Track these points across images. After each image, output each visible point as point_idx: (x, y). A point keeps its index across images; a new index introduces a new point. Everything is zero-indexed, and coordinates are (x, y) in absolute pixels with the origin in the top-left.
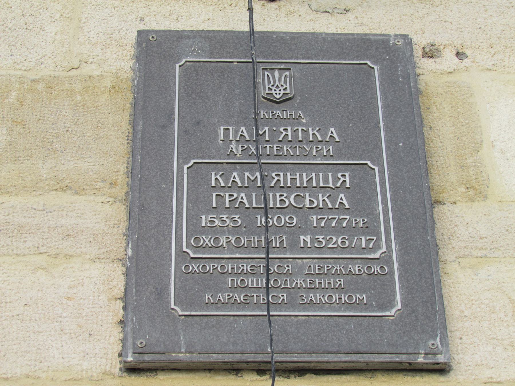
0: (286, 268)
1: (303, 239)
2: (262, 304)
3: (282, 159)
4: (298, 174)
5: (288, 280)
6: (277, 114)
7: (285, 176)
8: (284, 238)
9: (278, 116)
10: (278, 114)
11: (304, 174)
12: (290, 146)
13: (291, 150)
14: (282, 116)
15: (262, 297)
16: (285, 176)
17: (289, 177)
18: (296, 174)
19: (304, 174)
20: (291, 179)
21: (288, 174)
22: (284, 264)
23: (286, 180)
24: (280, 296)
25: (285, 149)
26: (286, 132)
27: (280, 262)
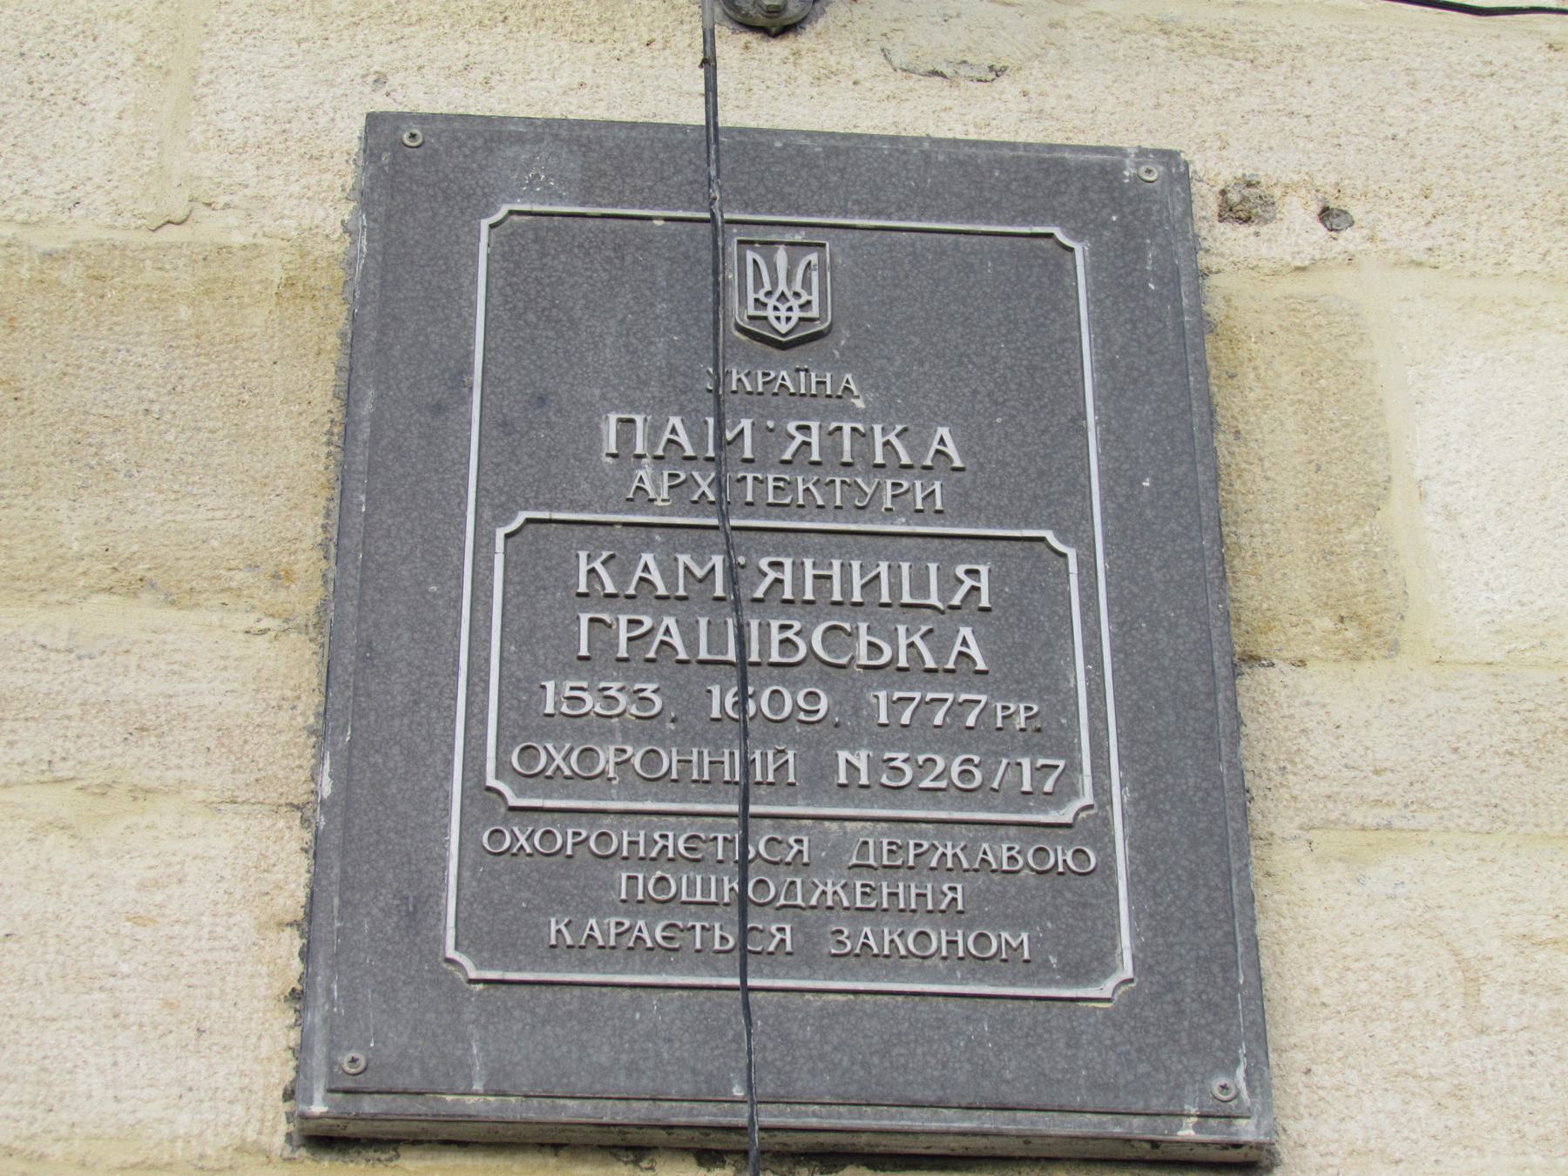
0: (792, 847)
1: (847, 761)
2: (719, 952)
3: (790, 518)
4: (836, 564)
5: (799, 882)
6: (779, 381)
7: (798, 567)
8: (790, 755)
9: (781, 385)
10: (783, 379)
11: (856, 565)
12: (815, 478)
13: (818, 490)
14: (794, 386)
15: (718, 933)
16: (798, 567)
17: (809, 572)
18: (831, 564)
19: (856, 565)
20: (816, 577)
21: (808, 563)
22: (789, 833)
23: (800, 582)
24: (773, 929)
25: (801, 487)
26: (805, 435)
27: (775, 829)
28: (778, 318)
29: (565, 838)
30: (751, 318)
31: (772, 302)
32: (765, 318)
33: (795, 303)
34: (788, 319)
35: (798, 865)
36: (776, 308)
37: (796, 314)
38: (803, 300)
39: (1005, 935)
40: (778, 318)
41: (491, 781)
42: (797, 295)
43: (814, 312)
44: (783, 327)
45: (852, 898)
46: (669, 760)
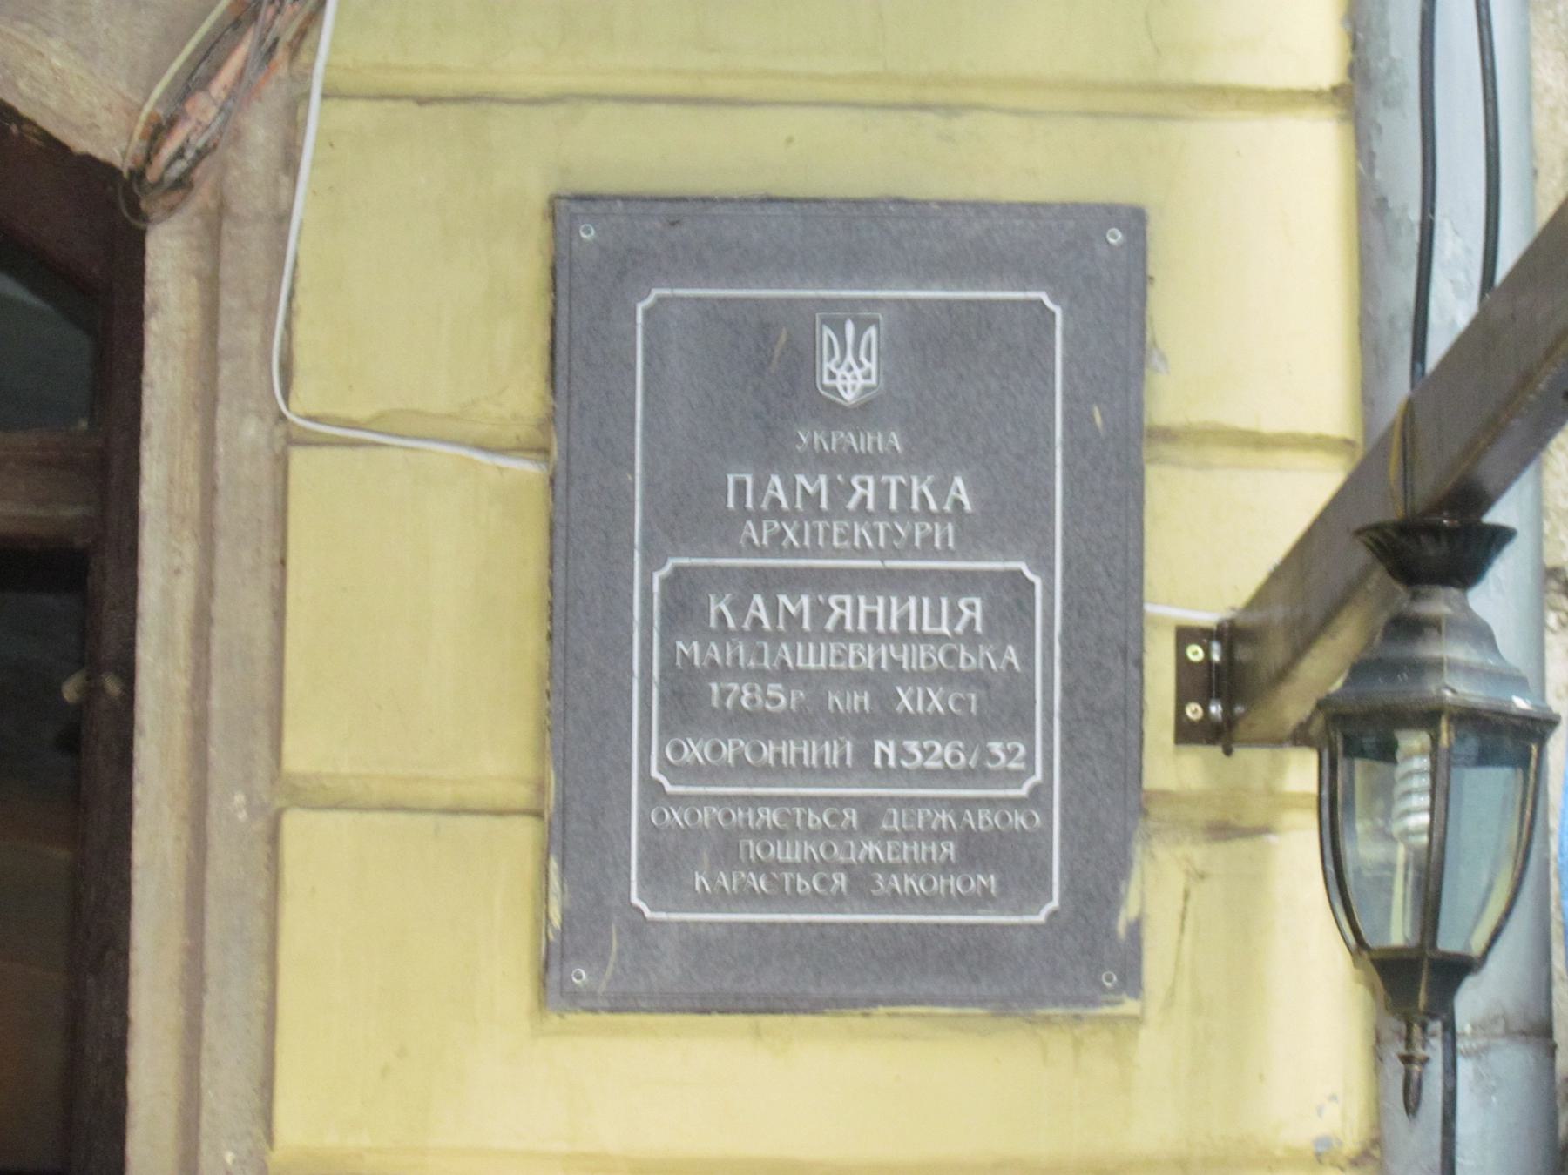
28: (845, 389)
29: (704, 816)
30: (823, 386)
31: (839, 373)
32: (835, 390)
33: (857, 371)
34: (854, 387)
35: (850, 832)
36: (844, 378)
37: (861, 382)
38: (864, 370)
39: (980, 878)
40: (845, 389)
41: (655, 774)
42: (860, 365)
43: (873, 381)
44: (849, 397)
45: (885, 855)
46: (768, 752)
